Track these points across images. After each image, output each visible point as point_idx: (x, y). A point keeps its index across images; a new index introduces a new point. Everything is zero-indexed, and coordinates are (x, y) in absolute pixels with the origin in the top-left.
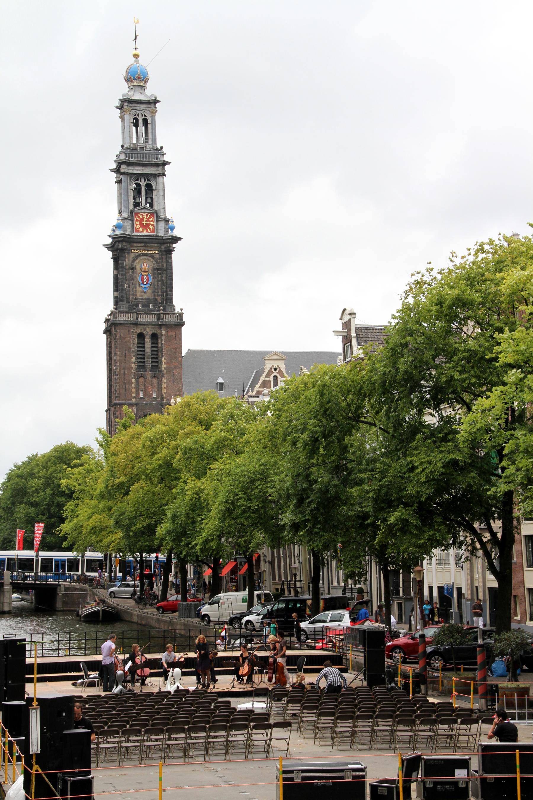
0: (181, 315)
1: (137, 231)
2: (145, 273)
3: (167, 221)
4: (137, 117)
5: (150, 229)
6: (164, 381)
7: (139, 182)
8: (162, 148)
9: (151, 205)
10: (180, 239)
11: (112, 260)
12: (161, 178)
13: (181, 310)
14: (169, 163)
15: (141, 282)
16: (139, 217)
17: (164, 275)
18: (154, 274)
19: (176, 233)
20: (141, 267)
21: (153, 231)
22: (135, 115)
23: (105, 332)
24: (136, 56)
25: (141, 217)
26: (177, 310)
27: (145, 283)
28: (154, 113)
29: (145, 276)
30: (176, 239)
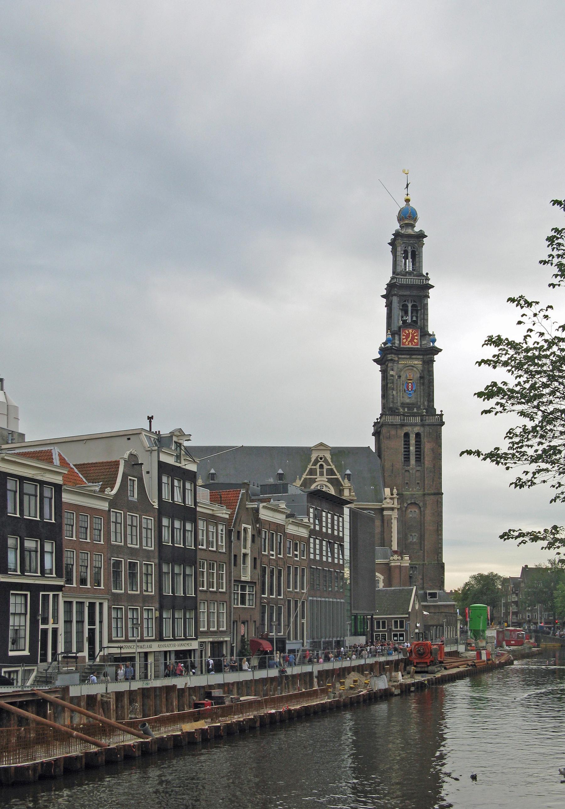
0: (441, 415)
1: (404, 344)
2: (410, 381)
3: (430, 335)
5: (414, 342)
7: (406, 303)
8: (427, 274)
10: (441, 350)
13: (441, 411)
14: (433, 287)
15: (406, 389)
16: (405, 333)
19: (437, 345)
20: (407, 375)
21: (417, 344)
22: (406, 248)
24: (407, 201)
25: (407, 333)
26: (438, 412)
27: (410, 390)
29: (410, 384)
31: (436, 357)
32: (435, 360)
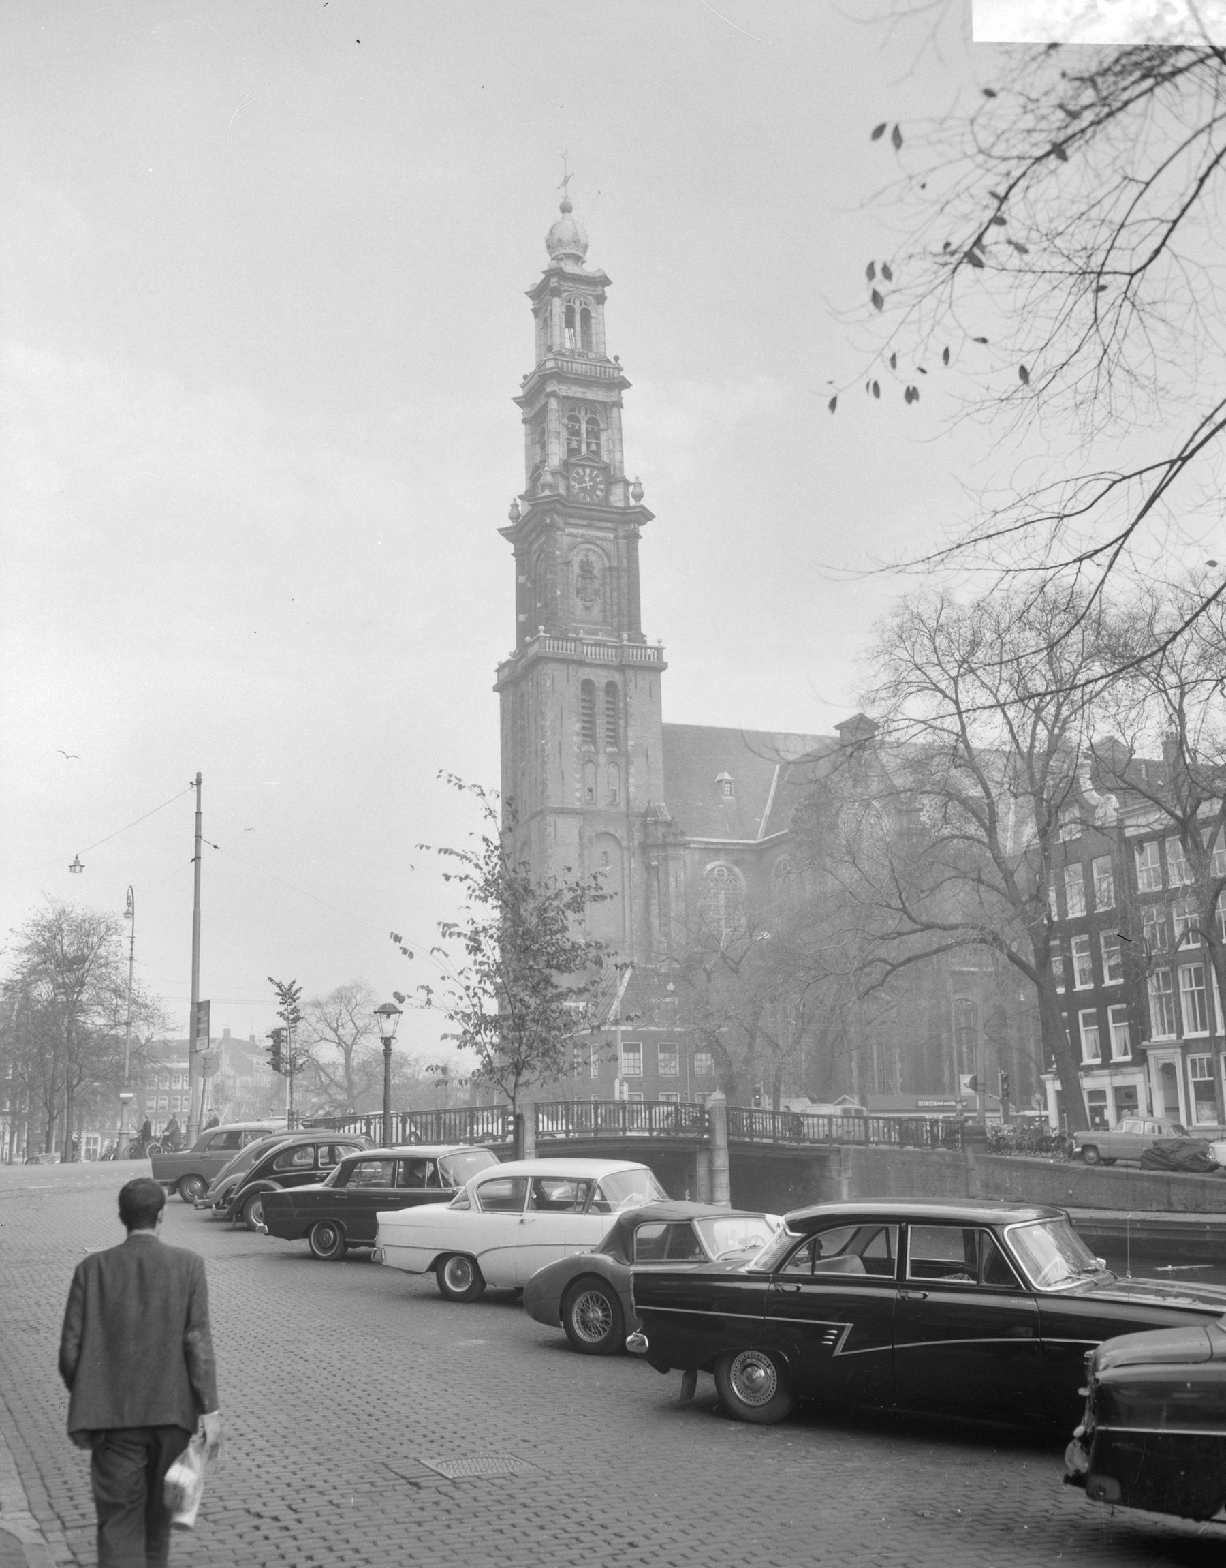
0: (659, 650)
3: (627, 484)
4: (572, 304)
5: (598, 496)
6: (632, 771)
8: (616, 358)
9: (597, 453)
11: (513, 559)
12: (615, 409)
13: (659, 642)
17: (624, 581)
18: (604, 577)
22: (569, 301)
23: (497, 688)
24: (566, 209)
28: (601, 299)
30: (646, 516)
31: (642, 530)
32: (640, 534)
